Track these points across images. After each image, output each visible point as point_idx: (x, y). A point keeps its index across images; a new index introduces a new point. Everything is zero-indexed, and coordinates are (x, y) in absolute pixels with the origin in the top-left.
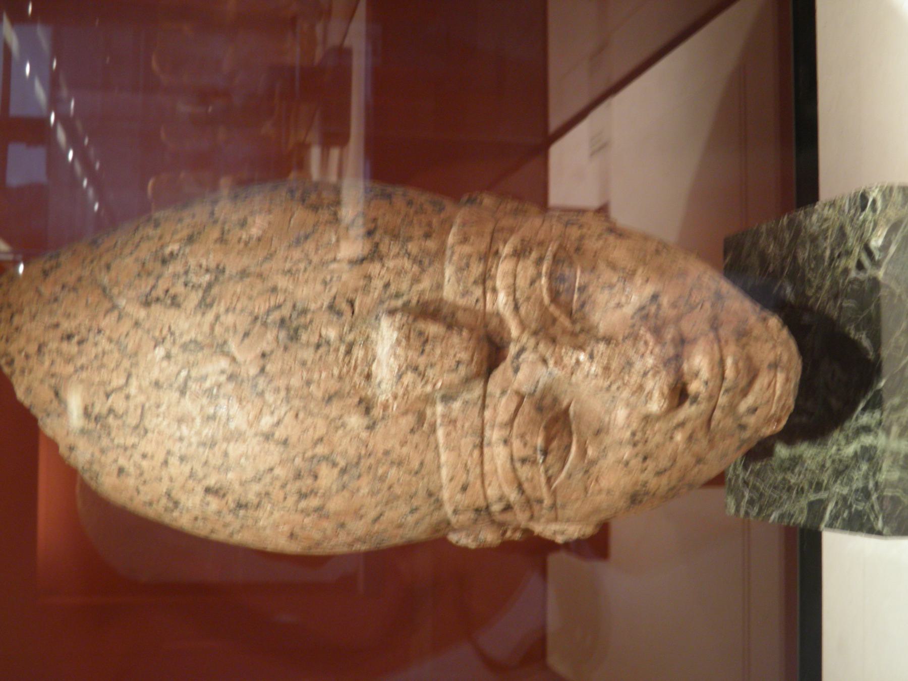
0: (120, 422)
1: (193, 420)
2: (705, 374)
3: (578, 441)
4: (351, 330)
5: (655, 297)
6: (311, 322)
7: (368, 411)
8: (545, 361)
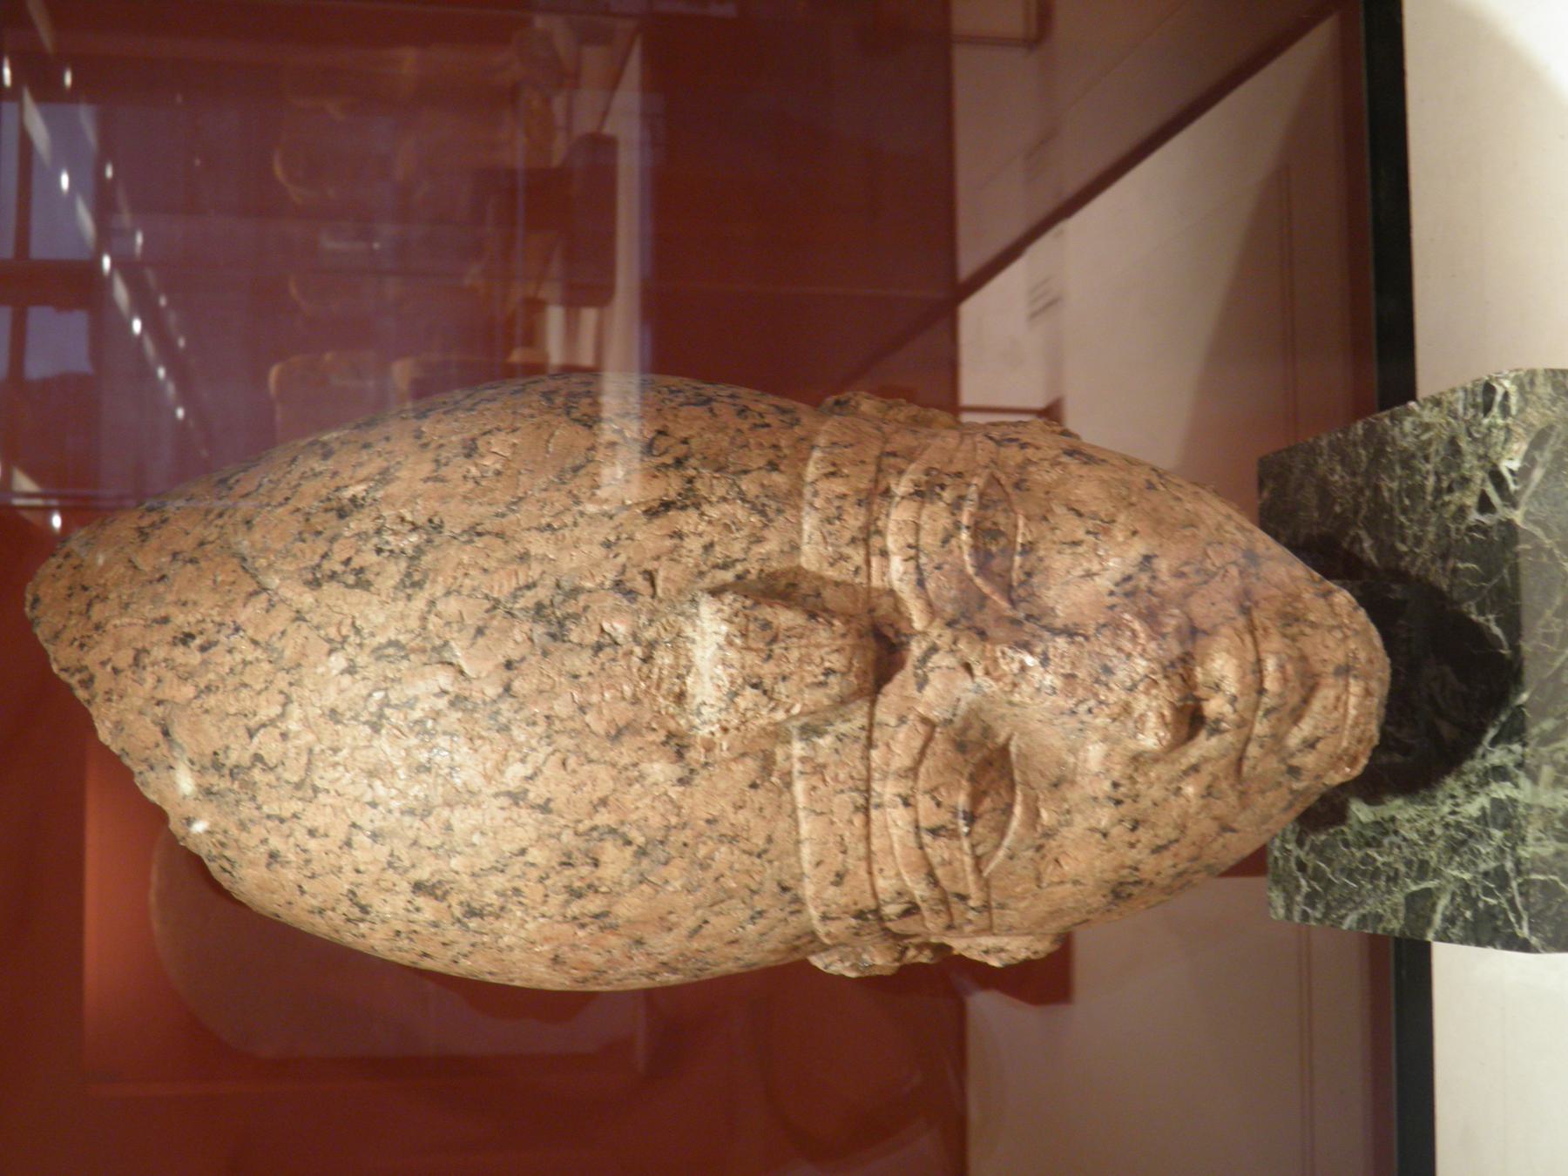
0: (271, 777)
1: (394, 771)
2: (1231, 687)
3: (1025, 796)
4: (651, 621)
5: (1147, 558)
6: (586, 608)
7: (680, 755)
8: (968, 668)
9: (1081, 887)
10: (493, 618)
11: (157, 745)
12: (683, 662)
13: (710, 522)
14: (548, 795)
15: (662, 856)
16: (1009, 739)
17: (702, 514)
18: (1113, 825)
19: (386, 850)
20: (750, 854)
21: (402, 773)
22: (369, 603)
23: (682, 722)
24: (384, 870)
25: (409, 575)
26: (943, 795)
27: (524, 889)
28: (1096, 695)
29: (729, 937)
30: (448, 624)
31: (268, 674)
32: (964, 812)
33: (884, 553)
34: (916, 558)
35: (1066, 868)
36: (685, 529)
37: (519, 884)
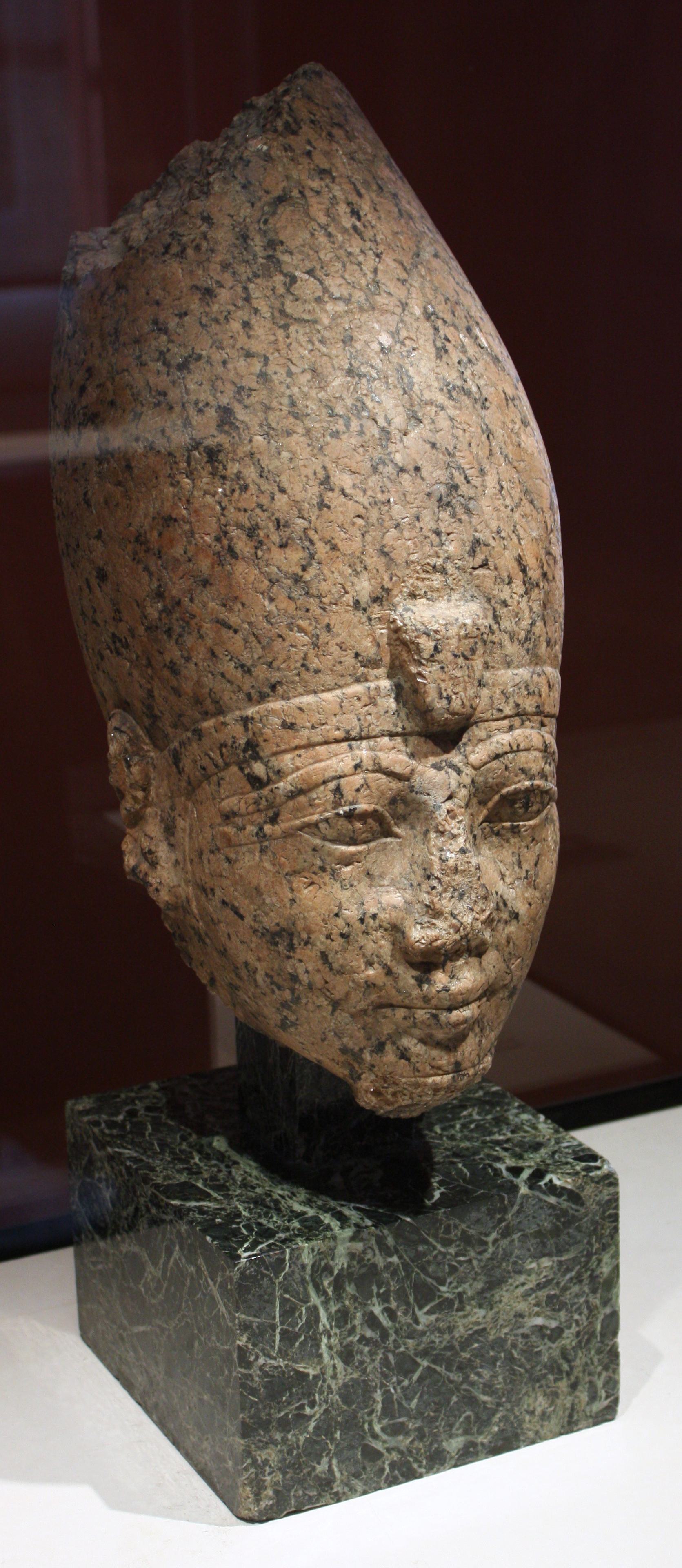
0: (281, 290)
1: (321, 388)
2: (455, 986)
3: (360, 852)
4: (458, 568)
5: (516, 916)
6: (460, 521)
7: (376, 600)
8: (450, 798)
9: (288, 905)
10: (443, 454)
11: (267, 192)
12: (435, 595)
13: (519, 603)
14: (332, 506)
15: (294, 595)
16: (396, 836)
17: (522, 596)
18: (344, 920)
19: (254, 385)
20: (304, 659)
21: (322, 395)
22: (429, 359)
23: (398, 599)
24: (234, 383)
25: (454, 388)
26: (364, 792)
27: (249, 493)
28: (445, 891)
29: (219, 651)
30: (433, 422)
31: (360, 284)
32: (355, 809)
33: (511, 728)
34: (512, 752)
35: (306, 891)
36: (514, 585)
37: (253, 489)
